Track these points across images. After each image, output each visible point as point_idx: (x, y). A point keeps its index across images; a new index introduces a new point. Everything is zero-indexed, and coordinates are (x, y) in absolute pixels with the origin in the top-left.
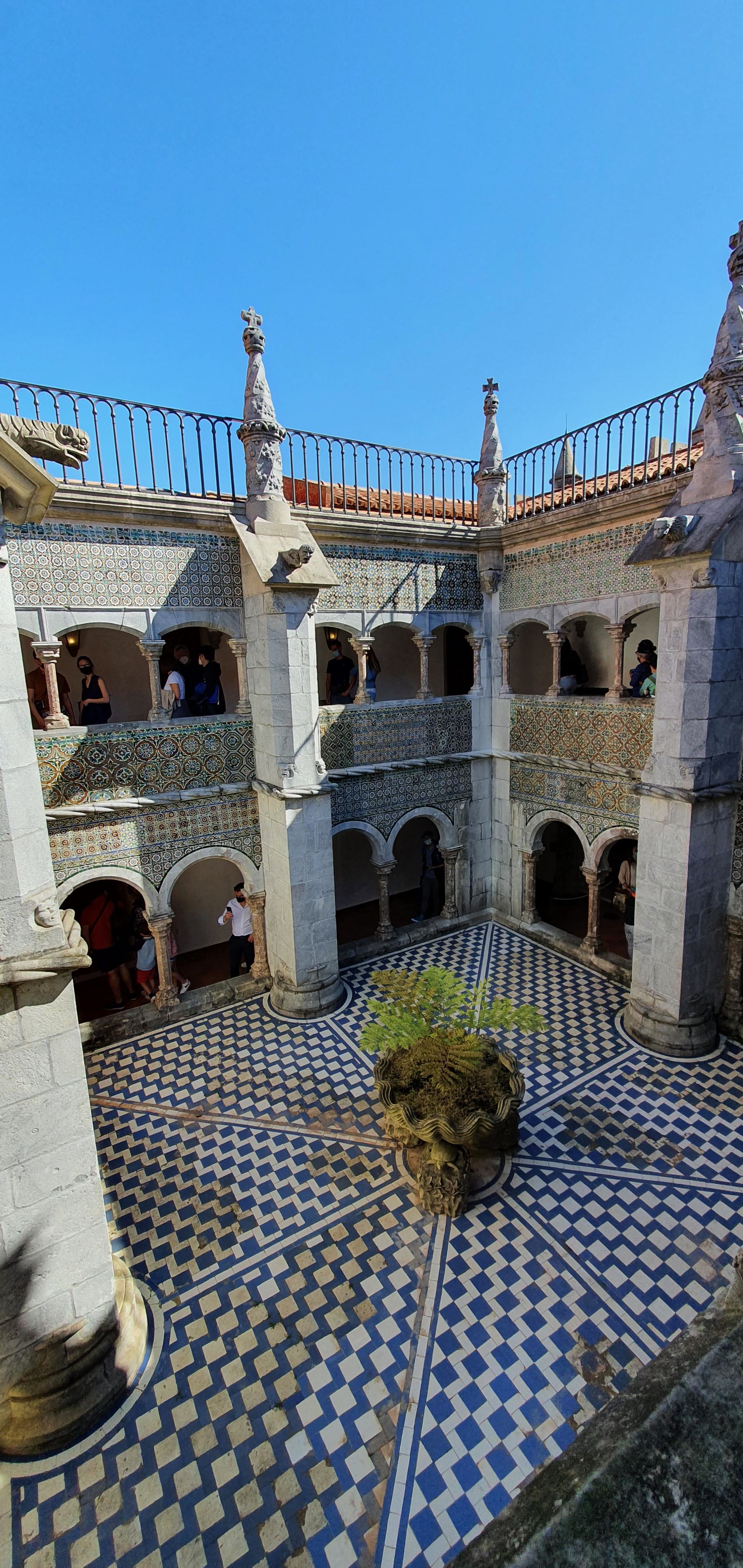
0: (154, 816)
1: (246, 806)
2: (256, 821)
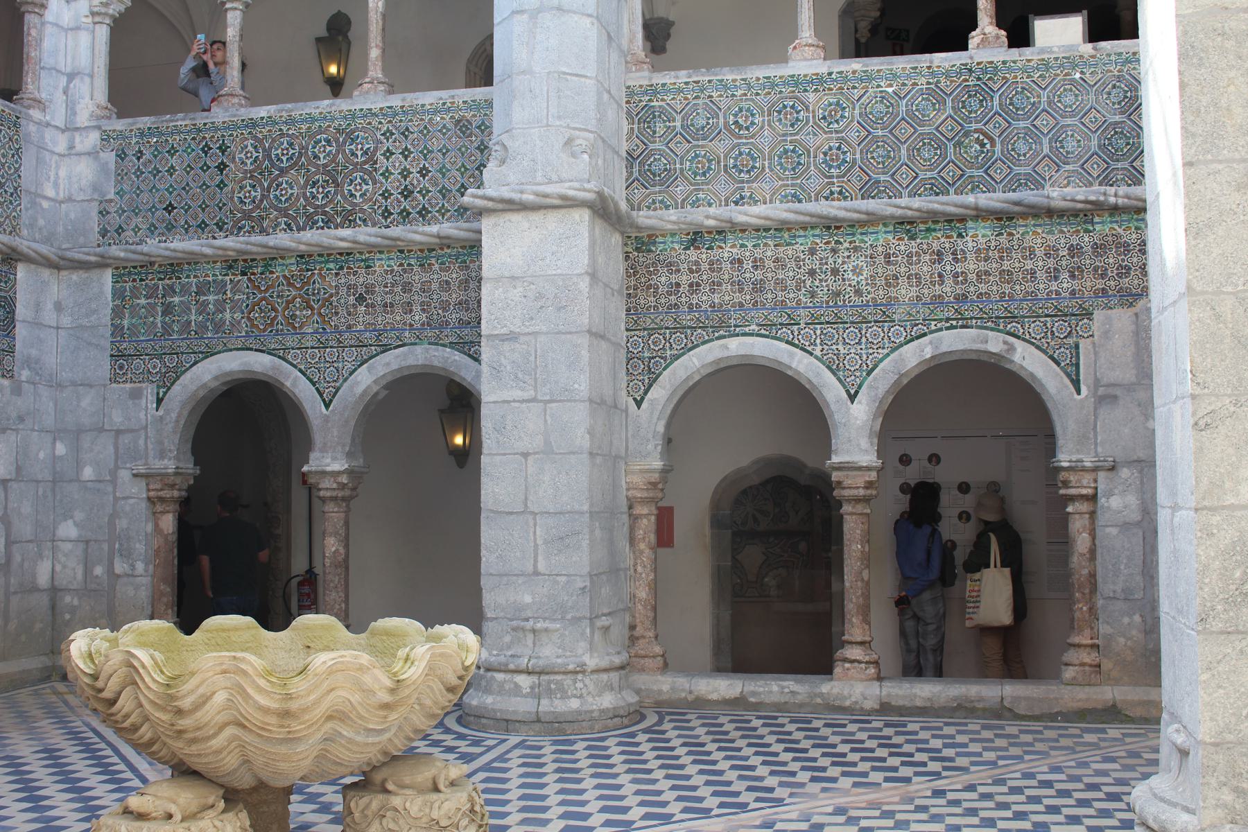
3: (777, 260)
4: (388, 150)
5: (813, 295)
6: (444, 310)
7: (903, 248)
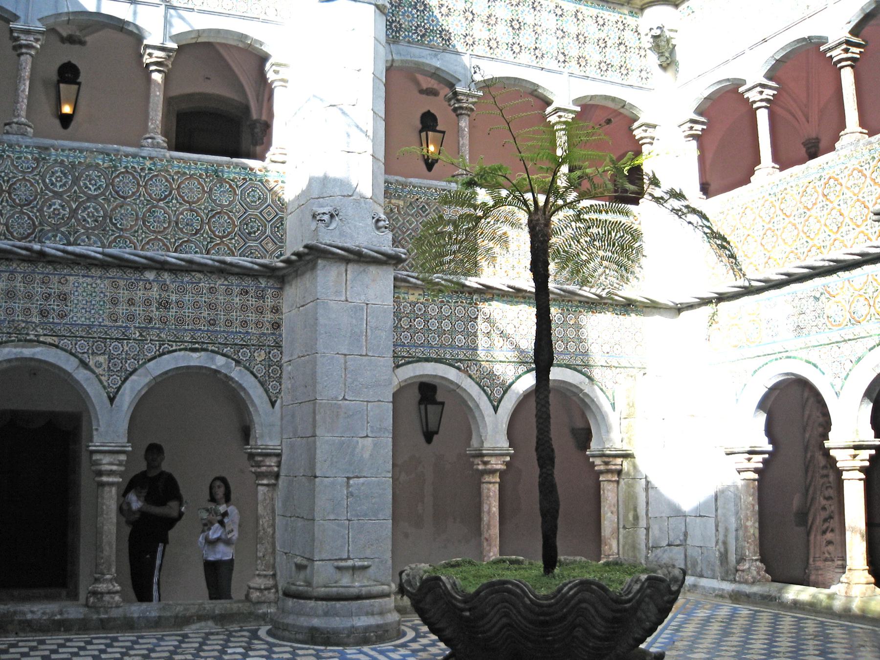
0: (122, 283)
1: (263, 297)
2: (276, 326)
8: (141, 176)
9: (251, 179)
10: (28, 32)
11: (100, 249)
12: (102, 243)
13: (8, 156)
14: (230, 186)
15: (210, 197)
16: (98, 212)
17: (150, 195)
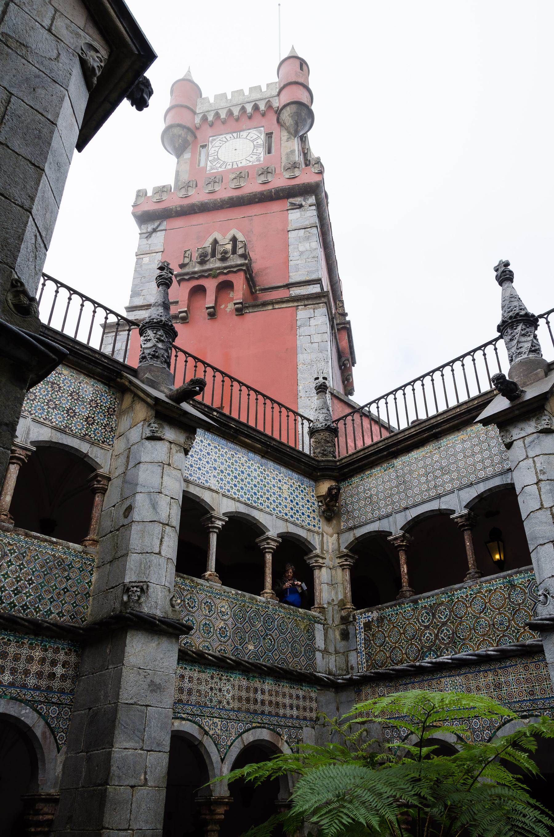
0: (470, 676)
3: (198, 679)
4: (10, 561)
5: (211, 701)
6: (26, 676)
7: (245, 683)
8: (467, 601)
9: (533, 579)
10: (396, 539)
11: (450, 657)
12: (455, 651)
13: (400, 612)
14: (521, 588)
15: (510, 601)
16: (449, 631)
17: (474, 611)
